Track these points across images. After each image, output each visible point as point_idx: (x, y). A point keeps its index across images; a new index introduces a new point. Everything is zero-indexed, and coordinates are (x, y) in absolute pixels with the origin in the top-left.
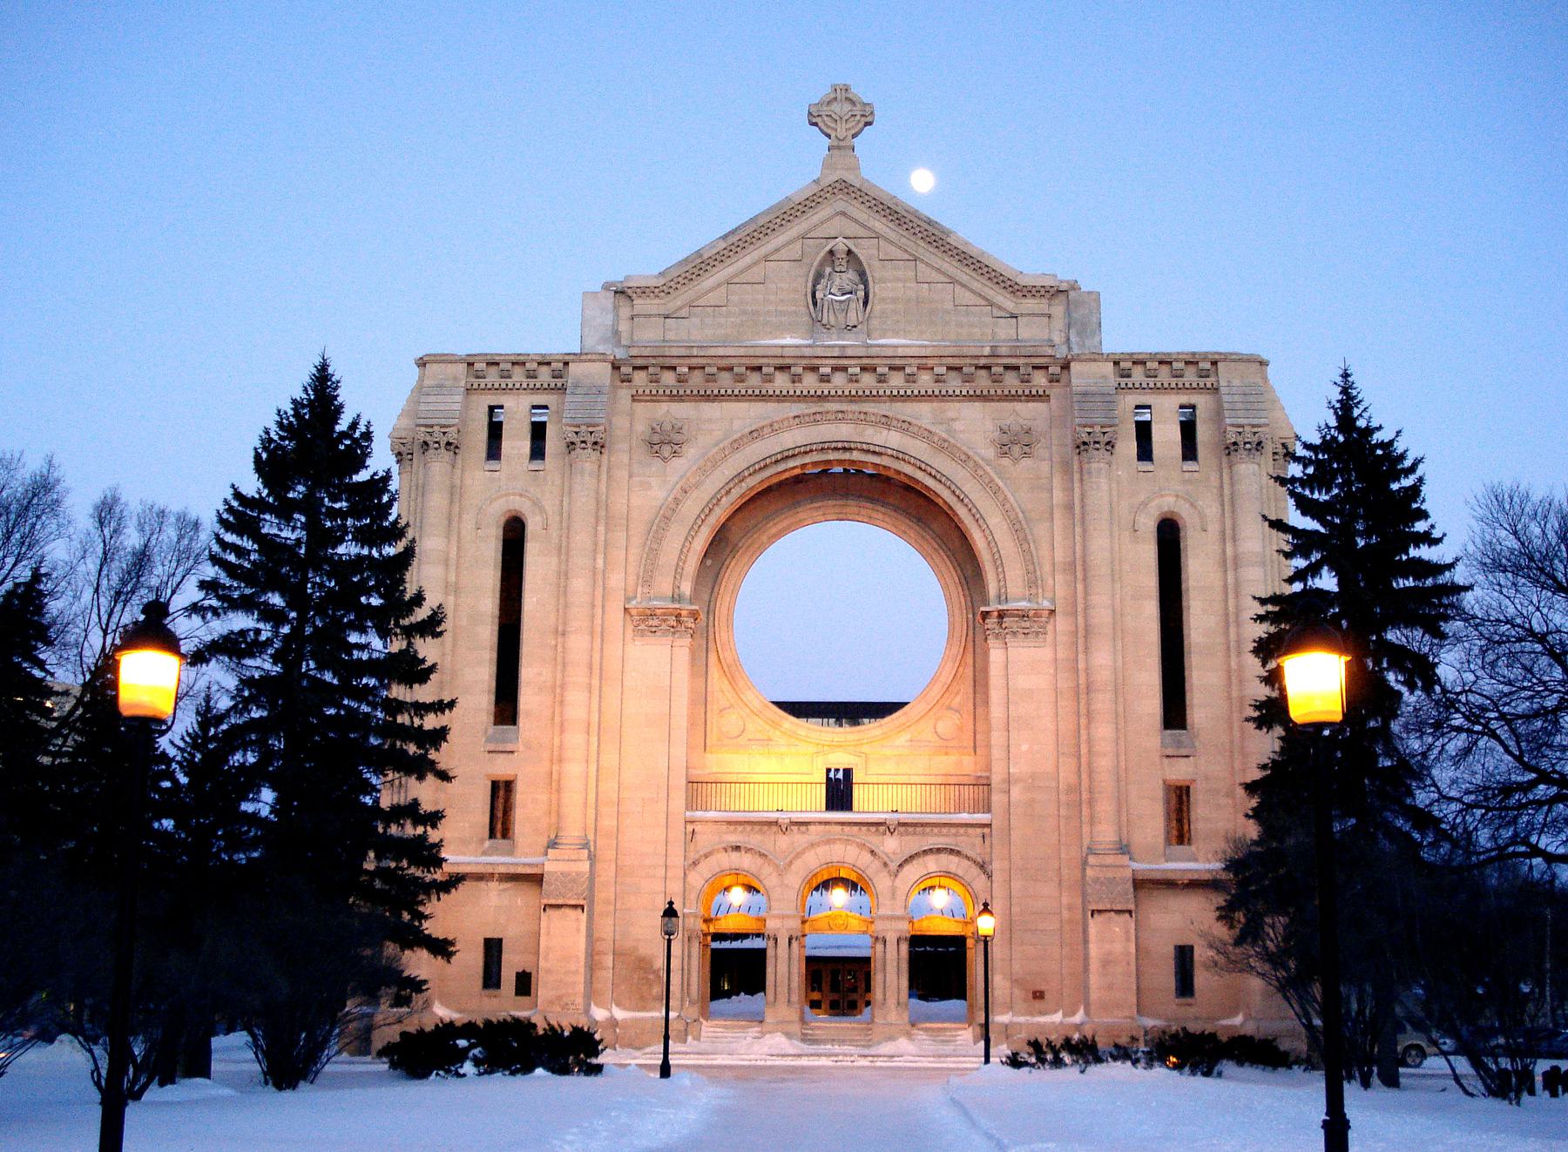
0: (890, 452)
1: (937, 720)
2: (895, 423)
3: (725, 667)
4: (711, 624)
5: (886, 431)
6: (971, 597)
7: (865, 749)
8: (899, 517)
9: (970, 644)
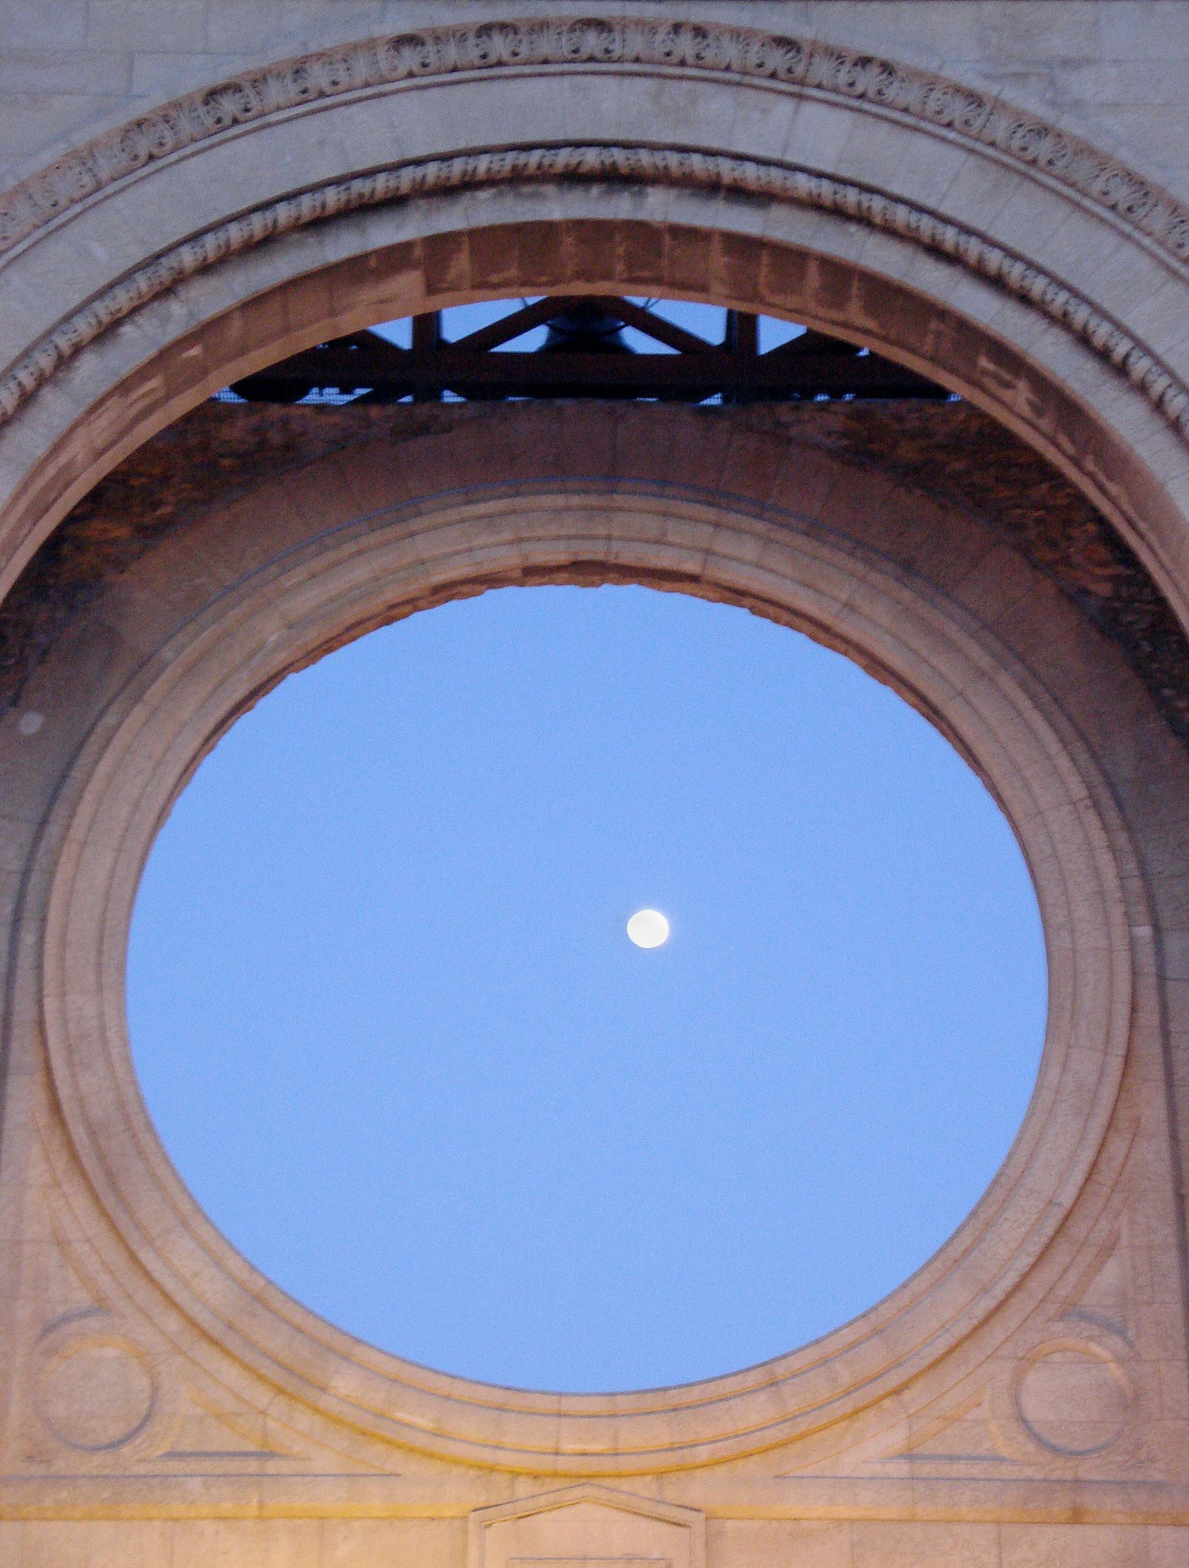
0: (803, 184)
1: (1026, 1362)
2: (822, 69)
3: (79, 1133)
4: (25, 961)
5: (785, 107)
6: (1142, 864)
7: (697, 1490)
8: (825, 552)
9: (1151, 1048)
